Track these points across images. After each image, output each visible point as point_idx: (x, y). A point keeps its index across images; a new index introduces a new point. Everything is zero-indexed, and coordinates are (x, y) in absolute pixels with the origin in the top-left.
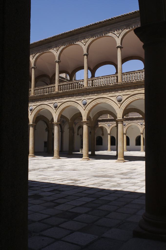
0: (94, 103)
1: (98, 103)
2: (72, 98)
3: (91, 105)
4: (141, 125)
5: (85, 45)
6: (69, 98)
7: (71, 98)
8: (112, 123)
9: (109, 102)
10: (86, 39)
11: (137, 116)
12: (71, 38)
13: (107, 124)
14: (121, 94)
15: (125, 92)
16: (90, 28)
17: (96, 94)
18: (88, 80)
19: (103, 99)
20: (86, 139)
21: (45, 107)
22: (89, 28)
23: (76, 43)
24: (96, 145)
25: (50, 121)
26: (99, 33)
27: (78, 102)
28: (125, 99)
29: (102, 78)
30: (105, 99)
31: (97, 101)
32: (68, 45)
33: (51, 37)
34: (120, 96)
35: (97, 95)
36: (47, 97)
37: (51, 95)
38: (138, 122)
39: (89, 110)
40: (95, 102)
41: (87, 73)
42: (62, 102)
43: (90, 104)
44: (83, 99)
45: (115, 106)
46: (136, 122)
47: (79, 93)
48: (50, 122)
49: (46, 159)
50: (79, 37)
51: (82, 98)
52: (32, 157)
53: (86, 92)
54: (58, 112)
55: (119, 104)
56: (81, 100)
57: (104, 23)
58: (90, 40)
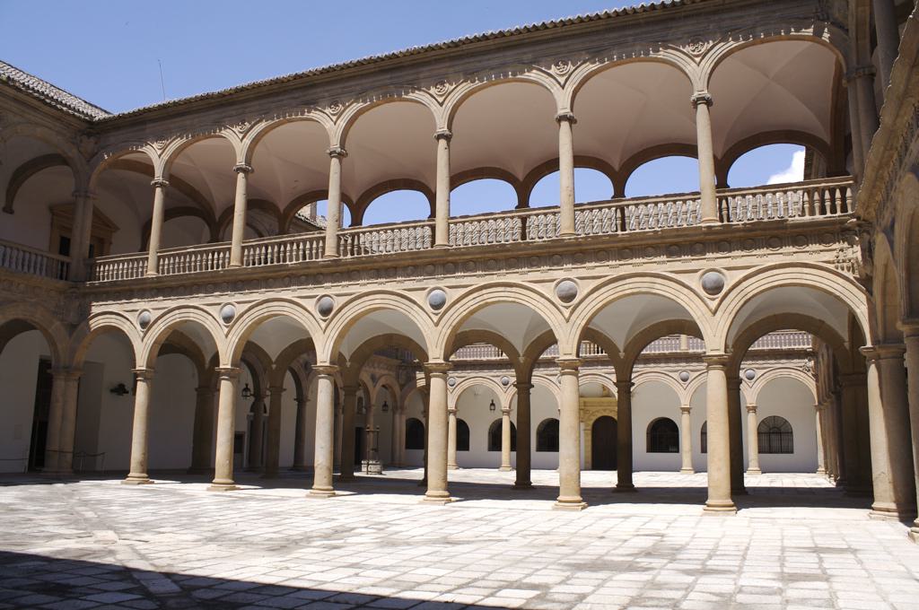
1: (489, 301)
2: (388, 280)
3: (461, 310)
4: (749, 379)
5: (441, 104)
6: (379, 280)
7: (384, 280)
8: (463, 375)
9: (530, 300)
10: (447, 85)
11: (697, 349)
12: (391, 78)
13: (497, 376)
14: (573, 274)
15: (589, 268)
17: (480, 273)
18: (450, 221)
19: (509, 289)
20: (439, 426)
21: (285, 309)
22: (458, 49)
23: (411, 94)
24: (539, 449)
25: (274, 360)
26: (492, 69)
27: (536, 289)
28: (586, 292)
29: (412, 227)
30: (514, 289)
31: (485, 297)
32: (378, 99)
33: (320, 68)
34: (569, 279)
36: (292, 274)
37: (309, 268)
38: (551, 373)
39: (453, 324)
40: (478, 299)
41: (447, 198)
42: (351, 294)
43: (458, 306)
44: (432, 286)
45: (552, 317)
46: (546, 372)
48: (274, 366)
49: (283, 499)
50: (421, 76)
51: (426, 284)
52: (226, 490)
53: (444, 265)
54: (336, 328)
55: (567, 308)
56: (424, 289)
57: (514, 38)
58: (460, 87)
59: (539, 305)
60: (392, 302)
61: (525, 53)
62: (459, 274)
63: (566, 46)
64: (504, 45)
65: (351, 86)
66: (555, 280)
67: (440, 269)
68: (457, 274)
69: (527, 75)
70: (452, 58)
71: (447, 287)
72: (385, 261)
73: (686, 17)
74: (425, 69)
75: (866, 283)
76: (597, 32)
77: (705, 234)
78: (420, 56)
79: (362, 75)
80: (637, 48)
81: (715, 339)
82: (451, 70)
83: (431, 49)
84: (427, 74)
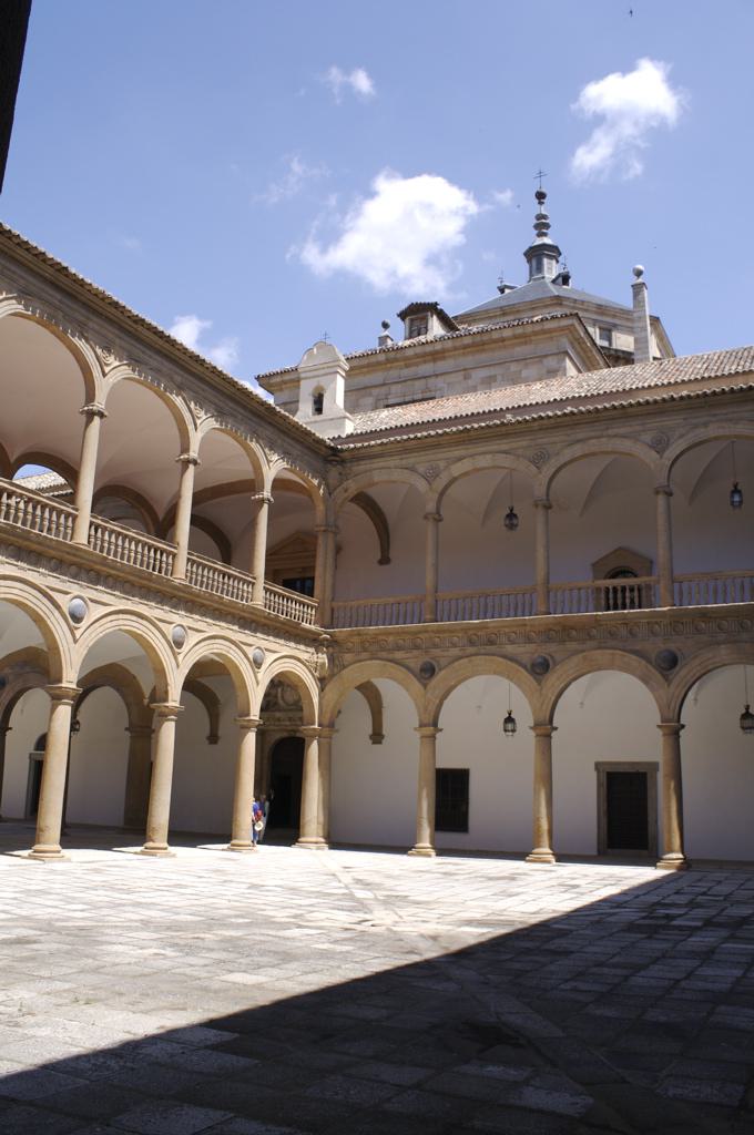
0: (109, 625)
6: (19, 563)
7: (25, 565)
10: (113, 357)
16: (136, 330)
19: (140, 620)
22: (135, 326)
30: (144, 622)
31: (121, 622)
34: (182, 626)
40: (114, 623)
43: (97, 625)
44: (76, 593)
47: (61, 562)
50: (91, 324)
57: (177, 353)
59: (160, 645)
60: (31, 598)
61: (177, 374)
65: (14, 272)
67: (83, 576)
68: (99, 587)
69: (173, 397)
70: (121, 328)
72: (40, 544)
73: (270, 423)
74: (95, 319)
75: (322, 682)
76: (223, 394)
77: (265, 618)
78: (101, 304)
79: (31, 270)
80: (242, 428)
81: (70, 679)
82: (117, 341)
83: (116, 305)
84: (96, 327)
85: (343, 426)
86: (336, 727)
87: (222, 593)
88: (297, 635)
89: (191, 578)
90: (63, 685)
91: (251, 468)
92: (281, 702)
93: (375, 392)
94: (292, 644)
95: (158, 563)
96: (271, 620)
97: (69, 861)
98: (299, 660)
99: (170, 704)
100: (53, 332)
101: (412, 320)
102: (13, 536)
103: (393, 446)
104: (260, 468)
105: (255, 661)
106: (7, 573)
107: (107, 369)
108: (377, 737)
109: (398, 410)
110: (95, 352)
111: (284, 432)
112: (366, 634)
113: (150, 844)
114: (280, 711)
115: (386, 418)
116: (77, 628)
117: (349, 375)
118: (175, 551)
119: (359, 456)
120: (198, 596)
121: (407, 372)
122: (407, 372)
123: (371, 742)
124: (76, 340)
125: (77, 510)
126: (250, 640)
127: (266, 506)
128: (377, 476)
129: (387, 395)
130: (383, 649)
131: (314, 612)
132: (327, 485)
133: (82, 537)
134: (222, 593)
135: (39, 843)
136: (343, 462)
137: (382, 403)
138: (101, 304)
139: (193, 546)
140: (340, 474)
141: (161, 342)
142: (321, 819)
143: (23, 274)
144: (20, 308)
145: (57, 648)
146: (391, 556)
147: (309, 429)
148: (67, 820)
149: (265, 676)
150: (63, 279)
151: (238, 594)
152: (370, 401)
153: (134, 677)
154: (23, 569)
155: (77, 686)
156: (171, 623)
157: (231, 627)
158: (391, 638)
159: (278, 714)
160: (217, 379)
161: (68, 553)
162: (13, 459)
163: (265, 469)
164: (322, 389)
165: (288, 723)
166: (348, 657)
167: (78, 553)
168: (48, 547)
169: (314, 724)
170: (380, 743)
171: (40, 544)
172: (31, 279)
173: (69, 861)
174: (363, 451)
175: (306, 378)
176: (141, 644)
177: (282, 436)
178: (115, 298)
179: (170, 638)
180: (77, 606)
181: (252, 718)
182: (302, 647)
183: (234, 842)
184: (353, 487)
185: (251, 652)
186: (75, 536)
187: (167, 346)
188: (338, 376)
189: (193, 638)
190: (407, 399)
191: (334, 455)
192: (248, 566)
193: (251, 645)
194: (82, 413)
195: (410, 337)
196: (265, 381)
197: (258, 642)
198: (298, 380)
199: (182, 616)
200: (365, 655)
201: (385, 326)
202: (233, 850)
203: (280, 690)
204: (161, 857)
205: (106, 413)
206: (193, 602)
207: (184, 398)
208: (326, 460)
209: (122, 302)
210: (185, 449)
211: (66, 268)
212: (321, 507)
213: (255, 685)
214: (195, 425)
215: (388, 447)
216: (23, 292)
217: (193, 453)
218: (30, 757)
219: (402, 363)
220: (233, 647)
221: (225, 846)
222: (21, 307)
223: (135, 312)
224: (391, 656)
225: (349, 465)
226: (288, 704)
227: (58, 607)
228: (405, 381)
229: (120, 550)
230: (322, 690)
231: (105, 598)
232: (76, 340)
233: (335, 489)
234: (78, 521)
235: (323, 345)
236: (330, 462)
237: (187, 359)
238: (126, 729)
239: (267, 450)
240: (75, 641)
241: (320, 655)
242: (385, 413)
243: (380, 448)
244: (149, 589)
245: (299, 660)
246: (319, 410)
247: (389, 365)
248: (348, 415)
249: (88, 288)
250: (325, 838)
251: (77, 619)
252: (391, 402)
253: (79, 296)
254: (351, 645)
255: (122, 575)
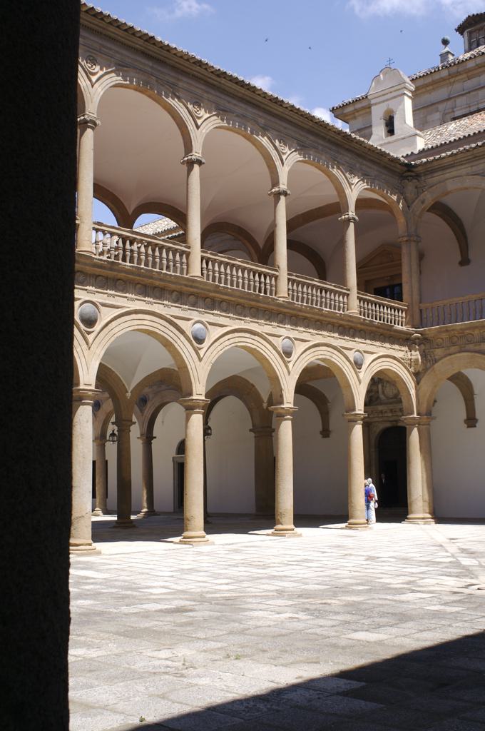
0: (227, 343)
6: (146, 299)
7: (151, 300)
16: (220, 83)
17: (232, 315)
19: (253, 337)
26: (237, 116)
30: (256, 338)
31: (237, 340)
32: (138, 84)
35: (237, 319)
40: (232, 341)
42: (118, 307)
43: (217, 344)
50: (180, 84)
51: (190, 315)
61: (261, 117)
62: (216, 312)
63: (285, 128)
64: (248, 99)
65: (110, 49)
66: (281, 336)
67: (201, 303)
69: (260, 138)
70: (207, 83)
71: (208, 322)
72: (161, 280)
73: (347, 150)
74: (185, 79)
75: (417, 376)
77: (361, 324)
78: (186, 64)
81: (199, 391)
82: (205, 95)
83: (199, 63)
85: (414, 143)
86: (433, 415)
87: (321, 306)
88: (390, 337)
89: (293, 296)
90: (194, 398)
91: (335, 193)
92: (382, 397)
93: (441, 107)
94: (387, 345)
95: (263, 285)
96: (367, 325)
97: (213, 544)
98: (394, 358)
99: (286, 405)
100: (150, 96)
101: (470, 33)
102: (139, 276)
103: (463, 155)
104: (344, 191)
105: (356, 363)
106: (138, 308)
107: (199, 122)
108: (471, 421)
109: (465, 121)
110: (187, 108)
111: (359, 155)
112: (453, 330)
113: (279, 527)
114: (381, 404)
115: (454, 130)
116: (200, 349)
117: (415, 96)
118: (277, 273)
119: (431, 169)
120: (300, 310)
121: (470, 84)
122: (470, 84)
123: (466, 426)
124: (170, 100)
125: (189, 248)
126: (350, 344)
127: (352, 225)
128: (451, 186)
129: (453, 108)
130: (470, 342)
131: (404, 315)
132: (405, 199)
133: (196, 270)
134: (321, 306)
135: (187, 530)
136: (417, 176)
137: (449, 117)
138: (186, 64)
139: (291, 267)
140: (416, 188)
141: (243, 90)
142: (427, 497)
143: (117, 49)
144: (119, 80)
145: (186, 367)
146: (471, 256)
147: (383, 150)
148: (208, 510)
149: (366, 375)
150: (152, 47)
151: (335, 305)
152: (437, 116)
153: (253, 386)
154: (150, 303)
155: (206, 397)
156: (279, 336)
157: (332, 335)
158: (476, 332)
159: (380, 408)
160: (296, 116)
161: (186, 285)
162: (130, 212)
163: (348, 191)
164: (392, 111)
165: (390, 415)
166: (439, 352)
167: (194, 284)
168: (169, 282)
169: (412, 413)
170: (475, 426)
171: (161, 280)
172: (124, 52)
173: (213, 544)
174: (435, 163)
175: (375, 104)
176: (256, 357)
177: (361, 160)
178: (198, 58)
179: (280, 349)
180: (198, 330)
181: (357, 412)
182: (397, 347)
183: (351, 521)
184: (429, 197)
185: (351, 355)
186: (190, 271)
187: (248, 93)
188: (406, 97)
189: (300, 347)
190: (473, 109)
191: (409, 171)
192: (342, 280)
193: (351, 349)
194: (183, 163)
195: (470, 49)
196: (339, 112)
197: (357, 346)
198: (369, 107)
199: (288, 329)
200: (453, 349)
201: (445, 42)
202: (350, 528)
203: (380, 386)
204: (289, 537)
205: (203, 161)
206: (297, 316)
207: (269, 138)
208: (402, 177)
209: (205, 60)
210: (275, 183)
211: (153, 38)
212: (401, 220)
213: (358, 383)
214: (282, 160)
215: (459, 156)
216: (120, 65)
217: (283, 186)
218: (173, 461)
219: (465, 76)
220: (335, 352)
221: (344, 525)
222: (120, 78)
223: (217, 67)
224: (477, 348)
225: (423, 178)
226: (387, 398)
227: (182, 332)
228: (469, 92)
229: (229, 278)
230: (418, 383)
231: (221, 320)
232: (170, 100)
233: (413, 203)
234: (192, 257)
235: (388, 70)
236: (406, 177)
237: (266, 102)
238: (251, 430)
239: (347, 175)
240: (200, 360)
241: (413, 352)
242: (452, 126)
243: (450, 159)
244: (258, 309)
245: (394, 358)
246: (391, 131)
247: (452, 80)
248: (418, 132)
249: (175, 52)
250: (430, 513)
251: (200, 340)
252: (457, 114)
253: (167, 60)
254: (441, 340)
255: (233, 299)
